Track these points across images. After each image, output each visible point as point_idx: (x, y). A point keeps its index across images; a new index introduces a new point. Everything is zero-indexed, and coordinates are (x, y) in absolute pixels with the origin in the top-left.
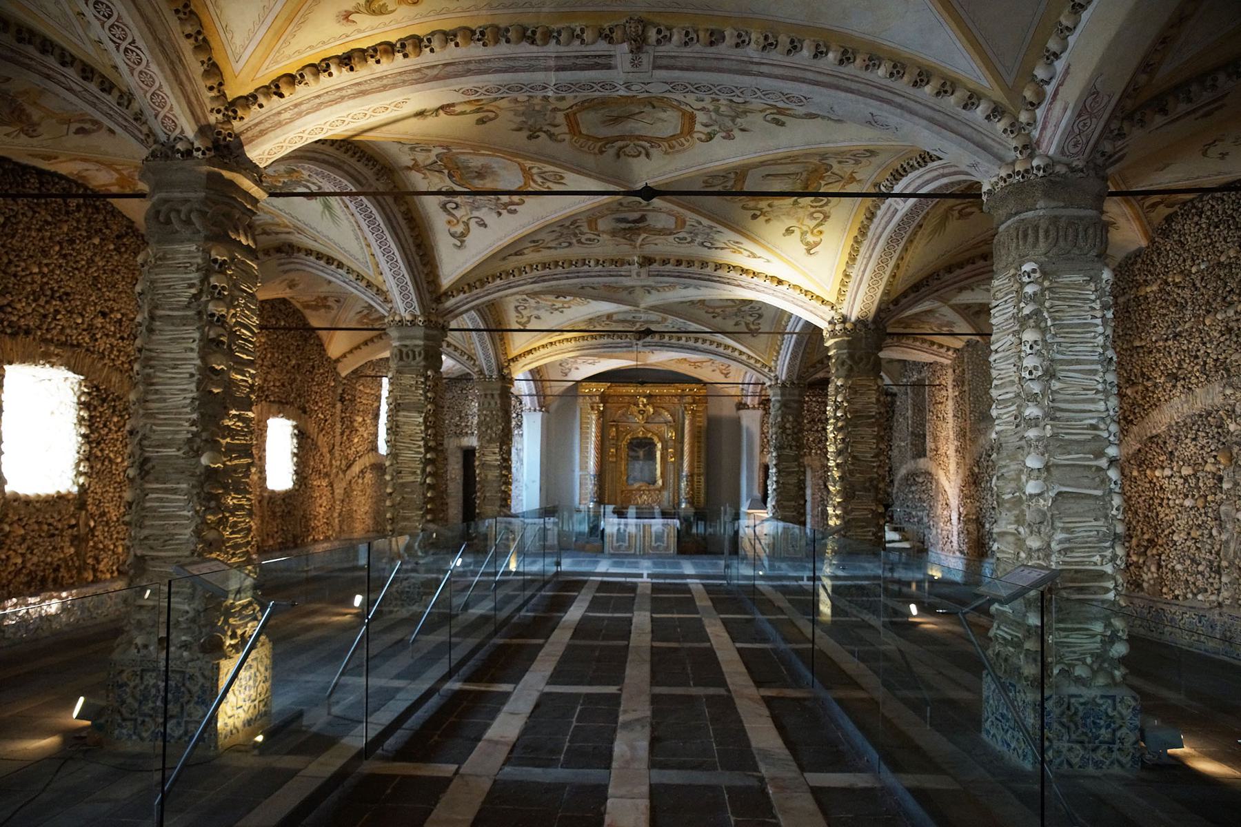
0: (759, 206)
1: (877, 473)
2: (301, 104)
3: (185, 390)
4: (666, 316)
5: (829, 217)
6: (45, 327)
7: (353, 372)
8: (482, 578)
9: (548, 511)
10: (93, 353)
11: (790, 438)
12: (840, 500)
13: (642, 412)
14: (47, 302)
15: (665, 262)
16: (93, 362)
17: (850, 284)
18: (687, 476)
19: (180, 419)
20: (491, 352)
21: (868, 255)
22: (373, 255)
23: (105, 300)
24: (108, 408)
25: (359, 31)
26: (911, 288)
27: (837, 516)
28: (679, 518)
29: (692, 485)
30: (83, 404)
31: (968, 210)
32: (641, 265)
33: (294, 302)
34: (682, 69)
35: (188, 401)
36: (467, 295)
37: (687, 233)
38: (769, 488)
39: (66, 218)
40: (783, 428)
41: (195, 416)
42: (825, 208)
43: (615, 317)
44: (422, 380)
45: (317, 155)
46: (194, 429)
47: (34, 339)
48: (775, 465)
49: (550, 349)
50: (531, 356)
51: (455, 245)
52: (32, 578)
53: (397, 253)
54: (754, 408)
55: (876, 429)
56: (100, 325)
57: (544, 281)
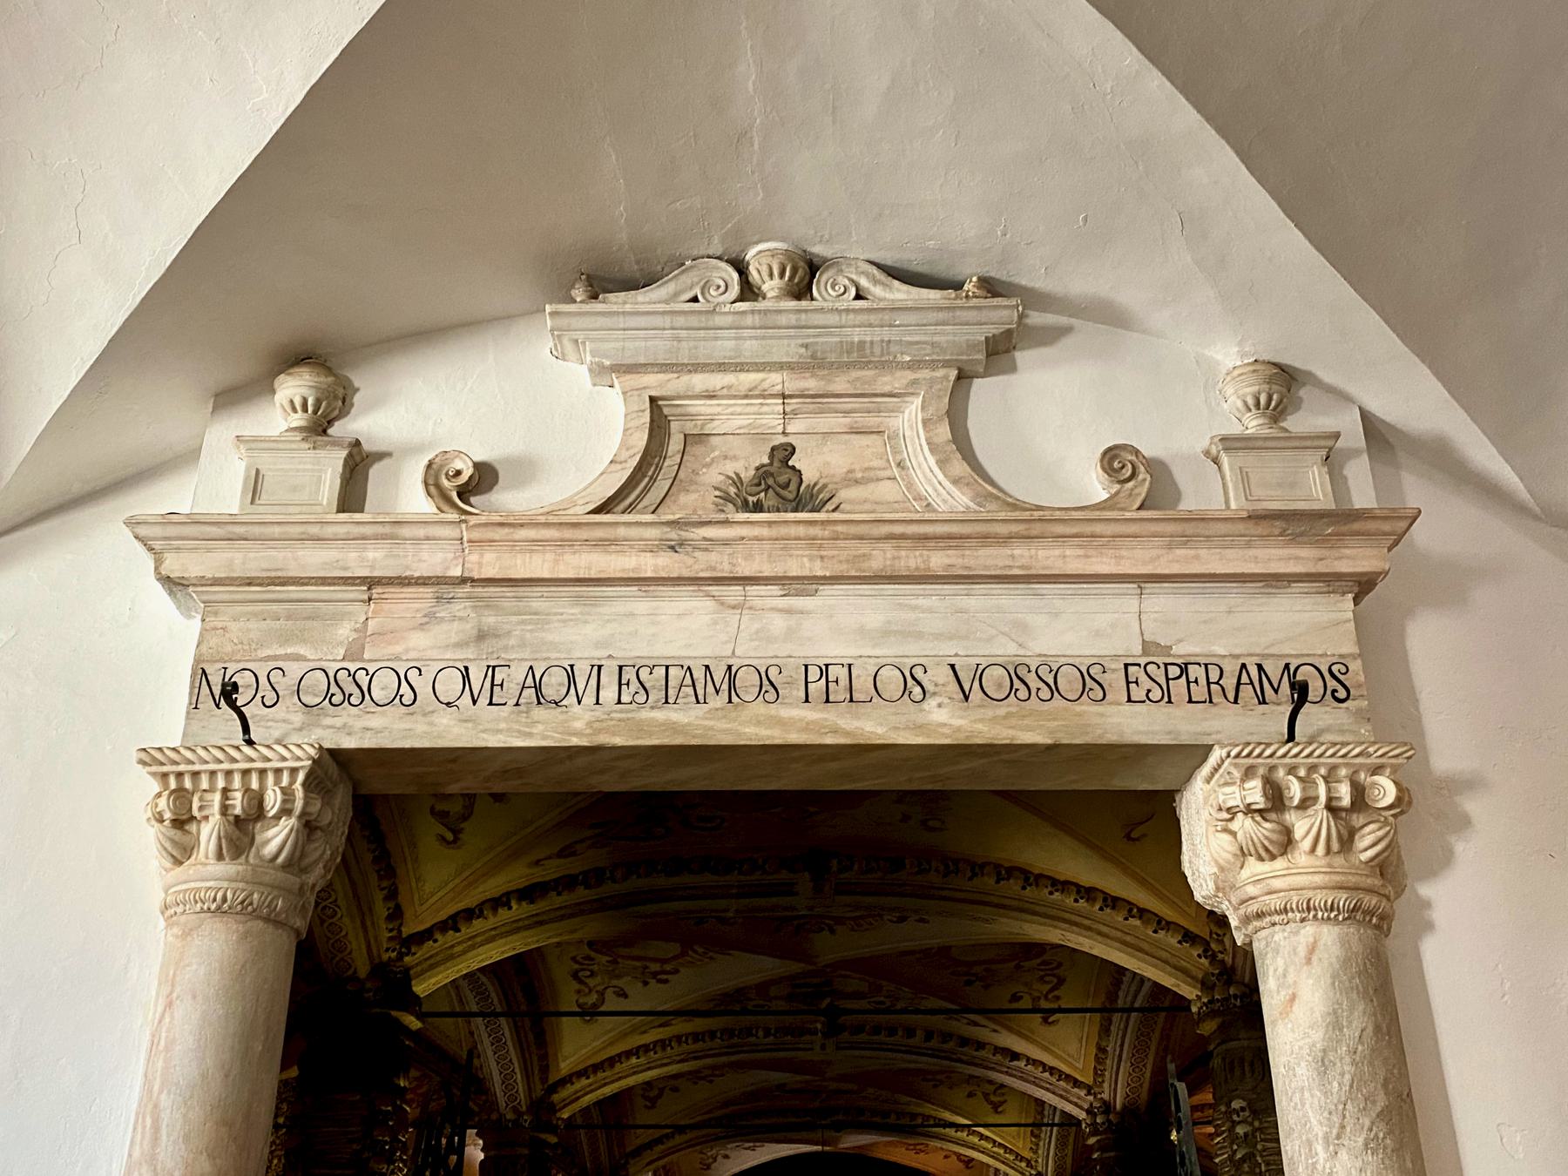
0: (973, 971)
2: (475, 936)
5: (1064, 980)
20: (602, 1148)
21: (1122, 1026)
25: (544, 870)
32: (826, 1035)
36: (590, 1081)
37: (886, 997)
42: (1059, 972)
50: (661, 1147)
53: (507, 1034)
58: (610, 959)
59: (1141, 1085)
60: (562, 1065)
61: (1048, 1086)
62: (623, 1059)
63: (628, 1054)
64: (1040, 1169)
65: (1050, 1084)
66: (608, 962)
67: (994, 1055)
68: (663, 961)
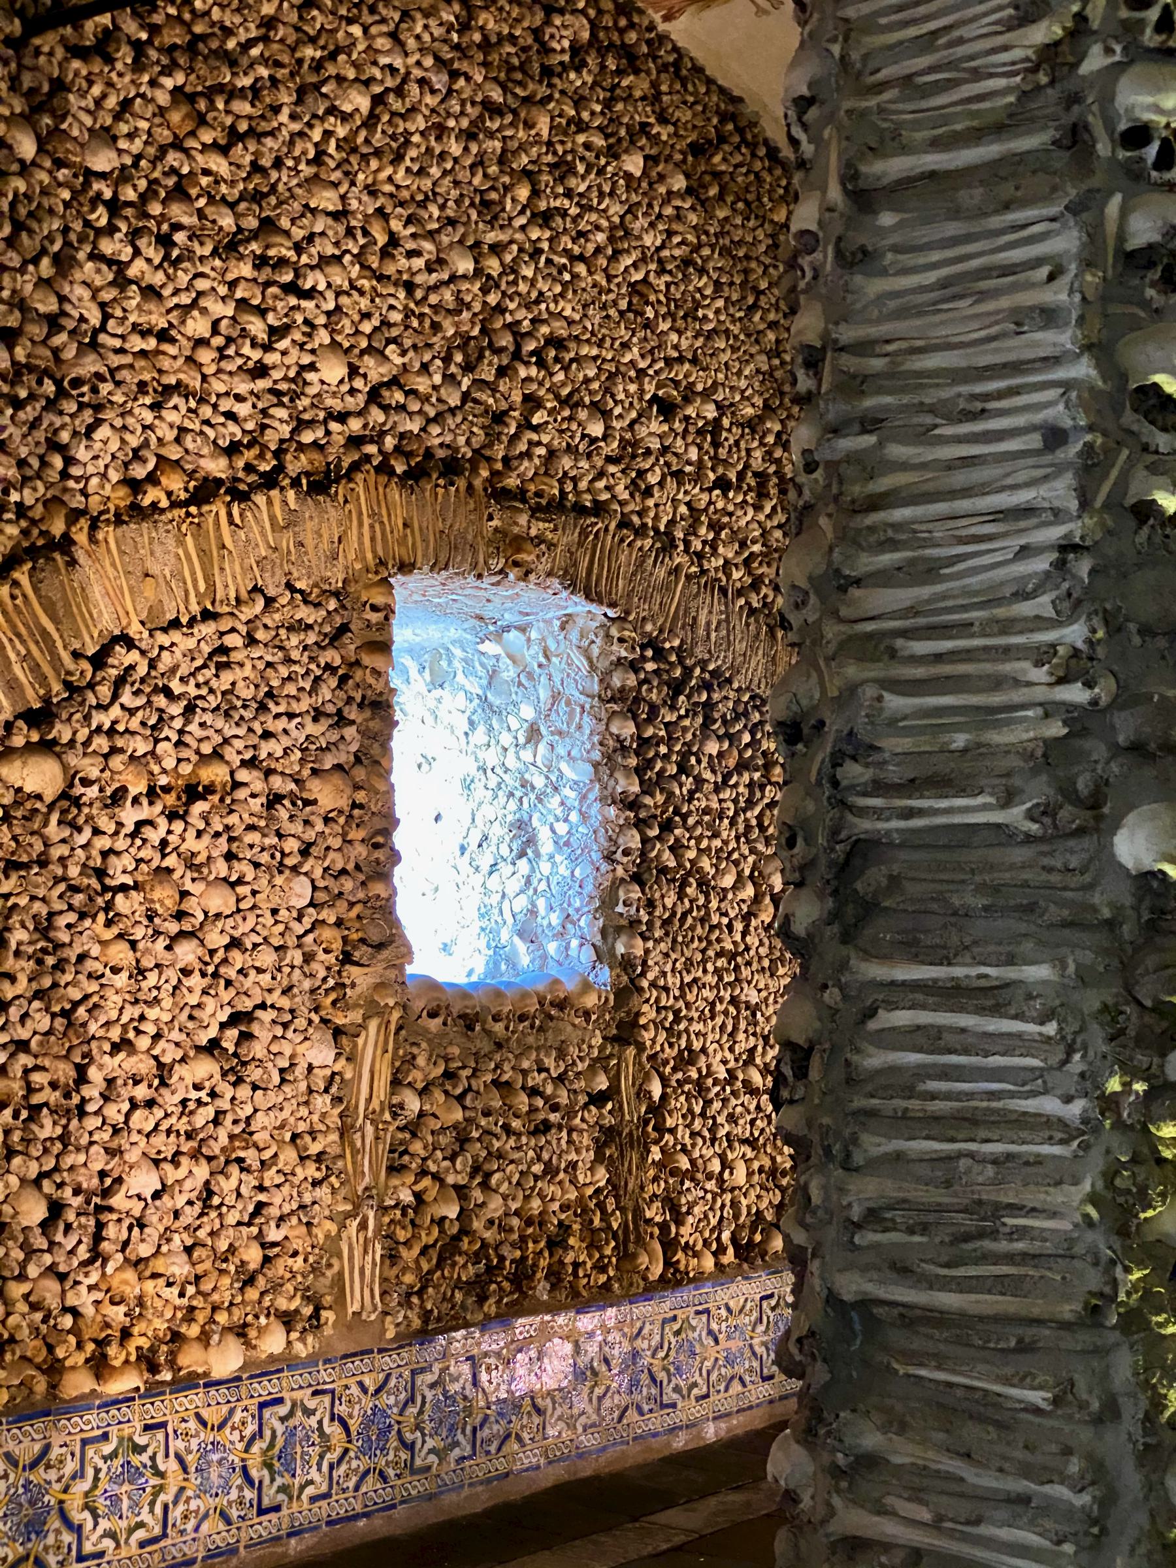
3: (1027, 511)
6: (499, 451)
10: (641, 531)
14: (502, 372)
16: (641, 563)
19: (1007, 652)
23: (669, 362)
24: (691, 713)
30: (619, 696)
35: (1041, 564)
39: (542, 91)
41: (1075, 634)
46: (1076, 694)
47: (470, 488)
52: (489, 1269)
56: (655, 444)
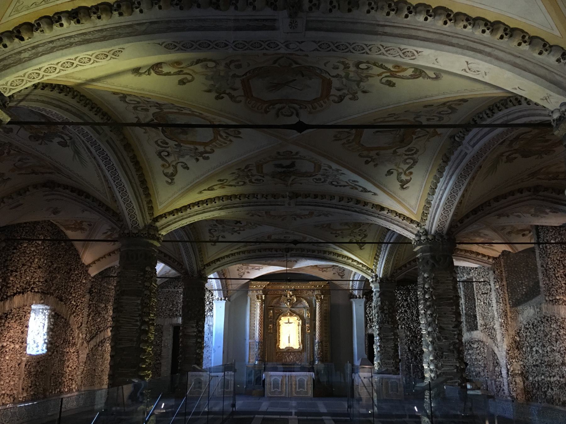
1: (457, 339)
4: (306, 235)
5: (417, 162)
7: (100, 274)
8: (177, 418)
9: (227, 367)
11: (387, 316)
12: (432, 358)
13: (290, 300)
15: (307, 196)
17: (430, 209)
18: (318, 341)
21: (443, 188)
22: (110, 188)
26: (471, 211)
27: (431, 371)
28: (314, 371)
29: (322, 349)
31: (514, 156)
32: (291, 198)
33: (58, 225)
34: (327, 30)
36: (175, 216)
37: (322, 175)
38: (375, 350)
40: (381, 309)
42: (415, 156)
43: (273, 237)
44: (142, 274)
45: (61, 104)
48: (378, 334)
49: (231, 258)
51: (167, 182)
54: (360, 297)
55: (454, 307)
57: (227, 208)
58: (177, 143)
59: (446, 221)
60: (160, 207)
61: (398, 223)
62: (191, 207)
63: (194, 204)
64: (377, 273)
65: (399, 222)
66: (175, 145)
67: (372, 208)
68: (205, 144)
